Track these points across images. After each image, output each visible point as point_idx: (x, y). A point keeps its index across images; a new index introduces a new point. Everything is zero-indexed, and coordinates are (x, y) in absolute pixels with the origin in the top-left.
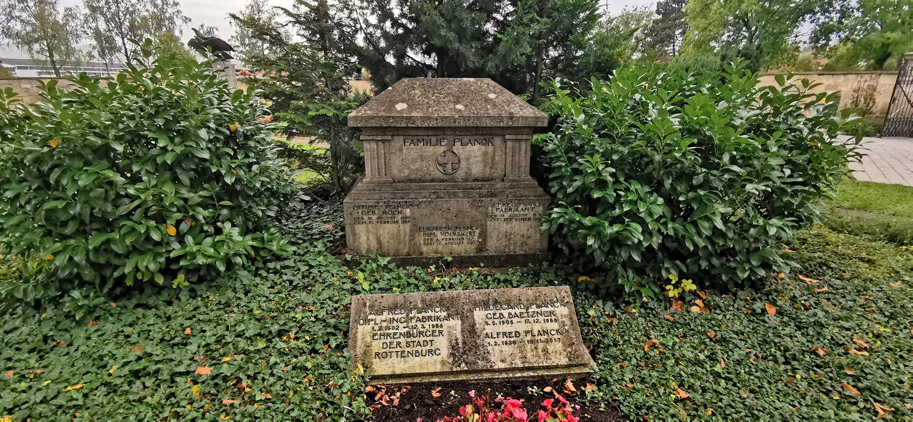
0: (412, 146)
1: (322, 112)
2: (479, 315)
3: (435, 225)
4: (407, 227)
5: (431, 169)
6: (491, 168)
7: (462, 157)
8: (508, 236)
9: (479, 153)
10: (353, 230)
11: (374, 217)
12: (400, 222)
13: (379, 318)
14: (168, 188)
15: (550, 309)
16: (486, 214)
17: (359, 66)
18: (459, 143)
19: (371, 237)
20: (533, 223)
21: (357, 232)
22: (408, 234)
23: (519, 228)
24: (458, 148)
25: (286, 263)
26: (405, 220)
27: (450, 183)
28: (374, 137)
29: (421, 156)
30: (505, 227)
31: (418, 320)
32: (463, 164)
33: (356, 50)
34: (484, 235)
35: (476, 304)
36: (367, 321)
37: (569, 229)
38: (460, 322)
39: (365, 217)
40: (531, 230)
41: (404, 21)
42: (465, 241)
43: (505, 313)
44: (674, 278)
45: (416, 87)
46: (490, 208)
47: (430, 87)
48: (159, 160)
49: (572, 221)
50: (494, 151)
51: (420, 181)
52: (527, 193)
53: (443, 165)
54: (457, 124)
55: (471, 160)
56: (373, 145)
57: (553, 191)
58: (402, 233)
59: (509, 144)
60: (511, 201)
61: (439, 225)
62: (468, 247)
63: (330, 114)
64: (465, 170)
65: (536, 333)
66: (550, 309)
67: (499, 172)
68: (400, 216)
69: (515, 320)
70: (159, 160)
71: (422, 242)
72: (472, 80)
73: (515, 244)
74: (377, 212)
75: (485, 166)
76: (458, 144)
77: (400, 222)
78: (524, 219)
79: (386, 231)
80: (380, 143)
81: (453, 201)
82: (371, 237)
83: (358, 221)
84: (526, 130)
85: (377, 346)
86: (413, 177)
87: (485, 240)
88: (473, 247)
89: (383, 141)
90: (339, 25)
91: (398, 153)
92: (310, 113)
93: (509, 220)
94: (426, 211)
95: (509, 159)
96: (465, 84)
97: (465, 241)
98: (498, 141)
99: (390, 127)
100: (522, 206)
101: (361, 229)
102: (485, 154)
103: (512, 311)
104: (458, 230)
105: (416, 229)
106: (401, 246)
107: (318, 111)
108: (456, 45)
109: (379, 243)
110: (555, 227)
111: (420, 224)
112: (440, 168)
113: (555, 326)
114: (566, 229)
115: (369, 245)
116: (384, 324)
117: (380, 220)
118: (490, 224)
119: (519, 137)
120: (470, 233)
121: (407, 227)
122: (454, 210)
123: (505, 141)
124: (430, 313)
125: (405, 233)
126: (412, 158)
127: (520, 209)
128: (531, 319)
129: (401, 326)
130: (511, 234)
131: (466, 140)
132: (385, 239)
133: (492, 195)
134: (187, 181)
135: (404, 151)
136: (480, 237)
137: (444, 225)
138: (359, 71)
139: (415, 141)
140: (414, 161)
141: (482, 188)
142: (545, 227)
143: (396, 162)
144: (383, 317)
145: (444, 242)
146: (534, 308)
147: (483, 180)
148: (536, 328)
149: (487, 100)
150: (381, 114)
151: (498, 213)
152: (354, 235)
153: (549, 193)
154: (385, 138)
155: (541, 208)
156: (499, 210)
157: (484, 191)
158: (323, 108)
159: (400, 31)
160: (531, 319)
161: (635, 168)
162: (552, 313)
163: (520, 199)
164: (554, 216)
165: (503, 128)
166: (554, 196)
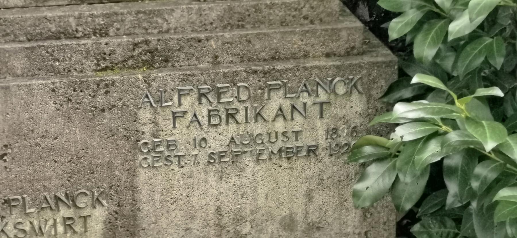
16: (133, 138)
20: (329, 166)
37: (464, 182)
46: (145, 115)
49: (475, 155)
52: (295, 43)
57: (396, 29)
60: (232, 79)
78: (288, 154)
100: (277, 100)
110: (412, 186)
114: (453, 187)
127: (270, 112)
133: (155, 58)
142: (376, 179)
151: (182, 133)
153: (382, 35)
155: (357, 104)
156: (185, 122)
157: (117, 44)
163: (268, 71)
164: (404, 134)
166: (403, 48)
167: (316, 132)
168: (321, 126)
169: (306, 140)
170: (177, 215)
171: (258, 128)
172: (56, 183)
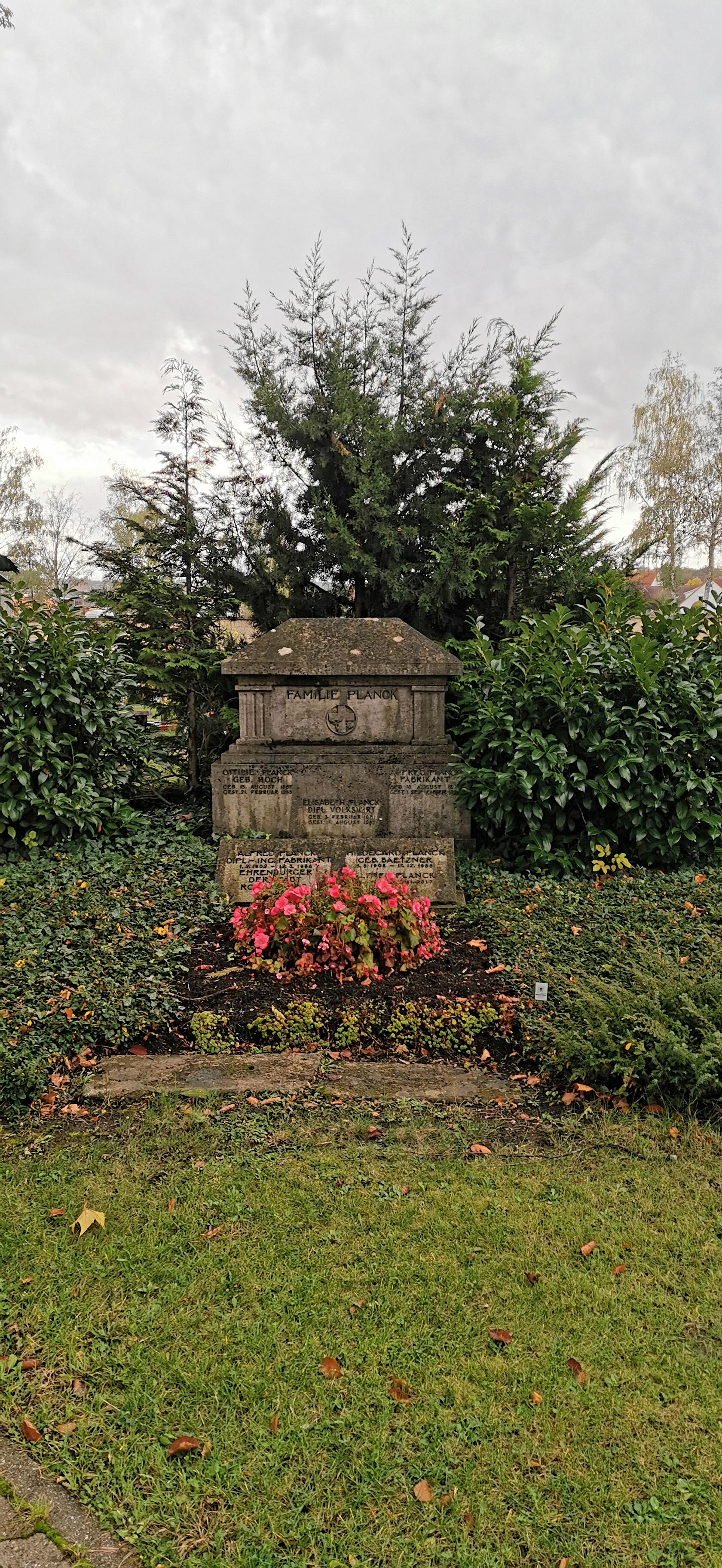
0: (298, 698)
1: (183, 663)
2: (350, 859)
3: (323, 798)
4: (288, 799)
5: (321, 728)
6: (396, 727)
7: (359, 713)
8: (417, 815)
9: (380, 708)
10: (221, 801)
11: (248, 785)
12: (280, 791)
13: (247, 858)
14: (36, 735)
15: (428, 856)
16: (389, 784)
17: (237, 601)
18: (355, 696)
19: (243, 811)
21: (226, 804)
22: (289, 808)
23: (431, 804)
24: (353, 702)
25: (137, 838)
26: (286, 789)
27: (342, 746)
28: (252, 688)
29: (308, 711)
30: (412, 802)
31: (287, 861)
32: (360, 722)
33: (233, 577)
34: (385, 812)
35: (349, 851)
36: (235, 860)
38: (330, 864)
39: (237, 785)
40: (446, 808)
41: (305, 532)
42: (362, 820)
43: (379, 858)
44: (604, 850)
45: (305, 629)
46: (392, 777)
47: (322, 629)
48: (34, 703)
50: (399, 706)
51: (308, 743)
53: (335, 723)
54: (350, 672)
55: (371, 718)
56: (251, 697)
58: (282, 806)
59: (417, 696)
61: (329, 797)
62: (366, 827)
63: (195, 666)
64: (363, 729)
65: (407, 875)
66: (428, 856)
67: (405, 733)
68: (280, 784)
69: (387, 864)
70: (34, 703)
71: (307, 820)
72: (376, 619)
73: (427, 826)
74: (251, 778)
75: (388, 725)
76: (354, 697)
77: (280, 791)
78: (437, 793)
79: (262, 804)
80: (258, 695)
81: (346, 768)
82: (243, 811)
83: (228, 789)
84: (438, 680)
85: (244, 879)
86: (296, 738)
87: (387, 819)
88: (373, 828)
89: (263, 692)
90: (210, 540)
91: (280, 707)
92: (167, 664)
93: (416, 793)
94: (312, 778)
95: (418, 716)
96: (366, 623)
97: (362, 820)
98: (403, 693)
99: (270, 675)
100: (433, 775)
101: (231, 800)
102: (388, 709)
103: (387, 857)
104: (352, 806)
105: (301, 802)
106: (281, 824)
107: (177, 661)
108: (374, 571)
109: (253, 818)
111: (304, 796)
112: (332, 727)
113: (430, 870)
115: (239, 822)
116: (252, 863)
117: (255, 790)
118: (394, 798)
119: (429, 688)
120: (368, 809)
121: (288, 799)
122: (347, 778)
123: (412, 693)
124: (300, 856)
125: (286, 806)
126: (297, 714)
127: (431, 779)
128: (405, 864)
129: (269, 865)
130: (421, 813)
131: (363, 692)
132: (260, 814)
133: (395, 761)
134: (50, 728)
135: (287, 705)
136: (381, 813)
137: (335, 797)
138: (235, 608)
139: (301, 693)
140: (299, 718)
141: (384, 752)
143: (277, 719)
144: (251, 858)
145: (334, 820)
146: (411, 855)
147: (385, 743)
148: (408, 872)
149: (391, 644)
150: (261, 659)
151: (403, 783)
152: (222, 807)
154: (264, 688)
156: (405, 779)
157: (386, 757)
158: (184, 658)
159: (301, 547)
160: (405, 864)
161: (547, 718)
162: (428, 859)
163: (431, 766)
165: (408, 677)
167: (445, 786)
168: (447, 784)
169: (442, 789)
170: (401, 810)
171: (427, 784)
172: (365, 797)
